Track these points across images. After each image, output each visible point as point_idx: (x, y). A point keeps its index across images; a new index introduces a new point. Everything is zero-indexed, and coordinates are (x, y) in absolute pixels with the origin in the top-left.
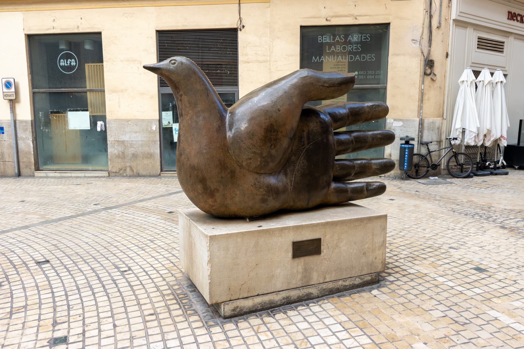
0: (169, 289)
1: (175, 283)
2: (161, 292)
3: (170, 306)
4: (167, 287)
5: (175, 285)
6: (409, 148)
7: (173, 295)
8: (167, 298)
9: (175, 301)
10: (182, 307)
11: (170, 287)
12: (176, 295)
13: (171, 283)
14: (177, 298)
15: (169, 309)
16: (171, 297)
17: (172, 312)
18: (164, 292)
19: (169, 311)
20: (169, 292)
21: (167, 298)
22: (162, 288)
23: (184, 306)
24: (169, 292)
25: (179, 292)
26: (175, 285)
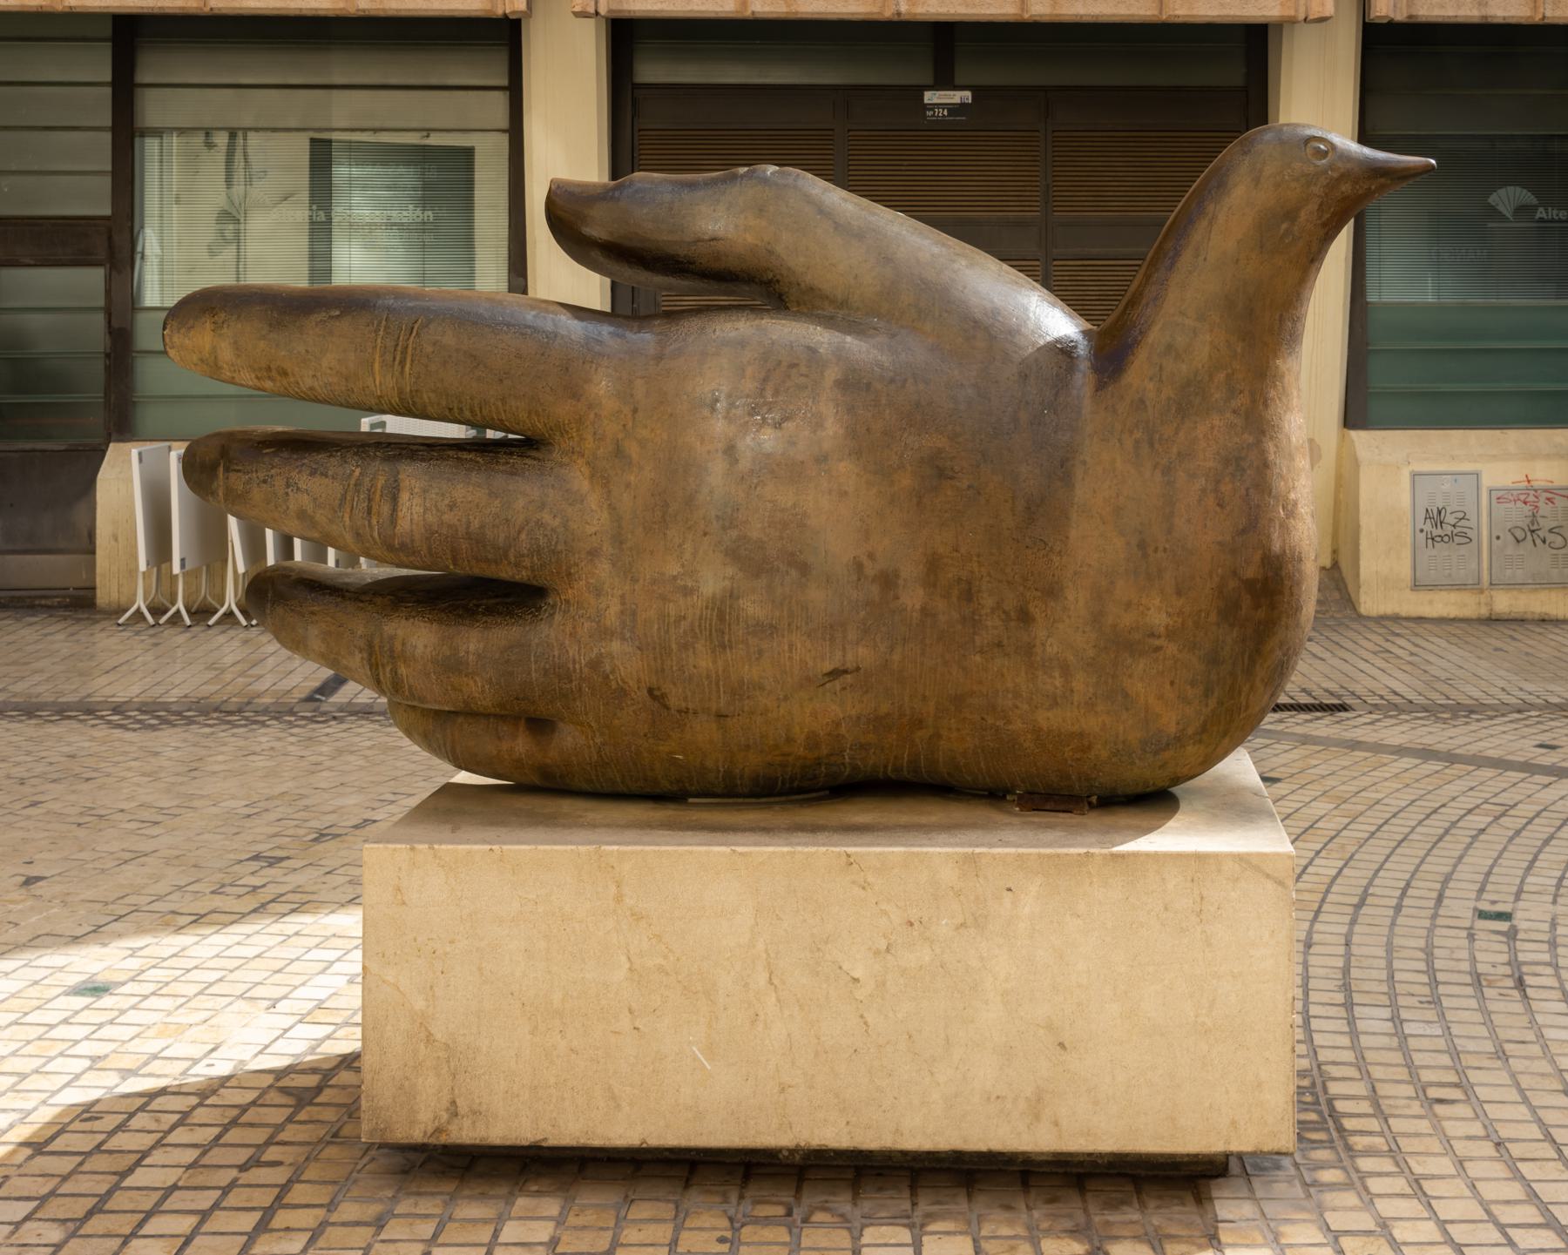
0: (1363, 1176)
1: (1330, 1198)
2: (1403, 1168)
3: (1371, 1111)
4: (1375, 1185)
5: (1332, 1187)
6: (854, 384)
7: (1348, 1148)
8: (1378, 1141)
9: (1348, 1124)
10: (1322, 1100)
11: (1357, 1182)
12: (1339, 1144)
13: (1350, 1198)
14: (1335, 1134)
15: (1376, 1104)
16: (1359, 1142)
17: (1364, 1092)
18: (1387, 1165)
19: (1374, 1098)
20: (1365, 1164)
21: (1378, 1141)
22: (1400, 1184)
23: (1317, 1103)
24: (1365, 1164)
25: (1322, 1155)
26: (1332, 1187)
